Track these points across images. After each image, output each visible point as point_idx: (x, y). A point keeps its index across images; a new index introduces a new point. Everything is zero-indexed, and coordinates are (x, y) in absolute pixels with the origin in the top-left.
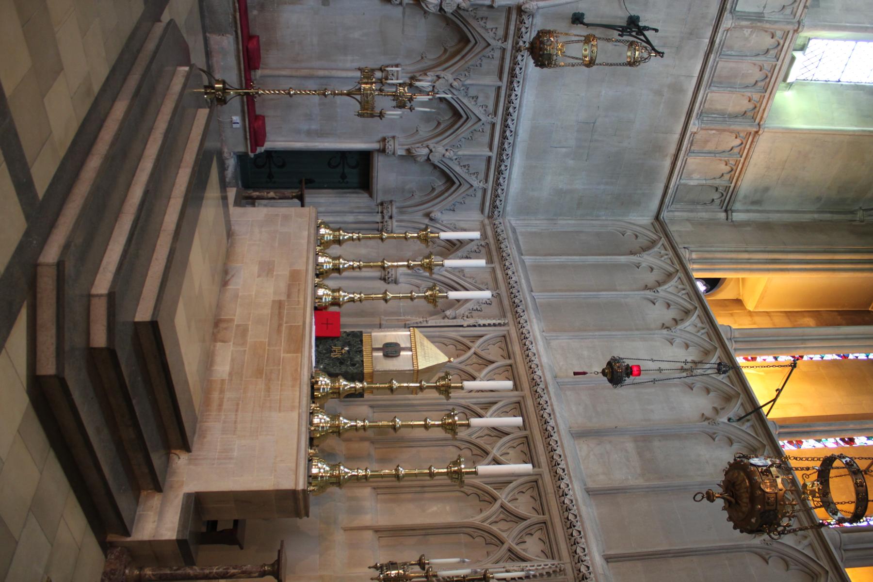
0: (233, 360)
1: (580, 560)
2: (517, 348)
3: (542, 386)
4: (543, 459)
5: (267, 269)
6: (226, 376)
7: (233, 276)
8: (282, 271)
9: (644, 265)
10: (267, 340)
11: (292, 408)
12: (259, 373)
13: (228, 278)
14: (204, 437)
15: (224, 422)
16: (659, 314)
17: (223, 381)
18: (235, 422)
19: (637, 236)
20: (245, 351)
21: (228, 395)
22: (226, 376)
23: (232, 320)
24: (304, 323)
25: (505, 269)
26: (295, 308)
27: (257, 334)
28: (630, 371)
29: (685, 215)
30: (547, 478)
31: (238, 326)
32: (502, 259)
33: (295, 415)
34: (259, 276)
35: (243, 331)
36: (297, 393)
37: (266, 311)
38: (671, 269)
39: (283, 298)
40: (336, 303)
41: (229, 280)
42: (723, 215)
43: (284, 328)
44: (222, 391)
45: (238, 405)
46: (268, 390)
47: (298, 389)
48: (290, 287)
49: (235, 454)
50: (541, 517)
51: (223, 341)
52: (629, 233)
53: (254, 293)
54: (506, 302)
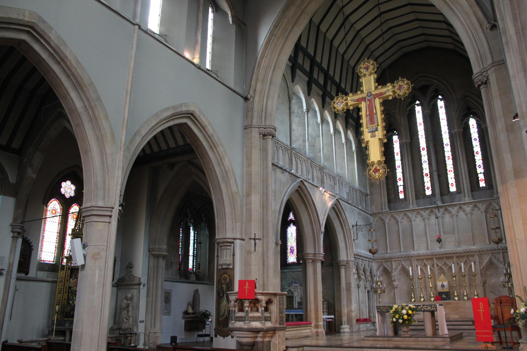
1: (476, 251)
2: (421, 258)
3: (433, 253)
9: (388, 222)
16: (405, 222)
19: (377, 221)
21: (463, 315)
22: (458, 316)
25: (395, 258)
28: (439, 238)
29: (369, 207)
30: (457, 255)
32: (392, 258)
38: (390, 215)
40: (433, 297)
42: (369, 197)
50: (465, 256)
52: (375, 223)
54: (406, 259)
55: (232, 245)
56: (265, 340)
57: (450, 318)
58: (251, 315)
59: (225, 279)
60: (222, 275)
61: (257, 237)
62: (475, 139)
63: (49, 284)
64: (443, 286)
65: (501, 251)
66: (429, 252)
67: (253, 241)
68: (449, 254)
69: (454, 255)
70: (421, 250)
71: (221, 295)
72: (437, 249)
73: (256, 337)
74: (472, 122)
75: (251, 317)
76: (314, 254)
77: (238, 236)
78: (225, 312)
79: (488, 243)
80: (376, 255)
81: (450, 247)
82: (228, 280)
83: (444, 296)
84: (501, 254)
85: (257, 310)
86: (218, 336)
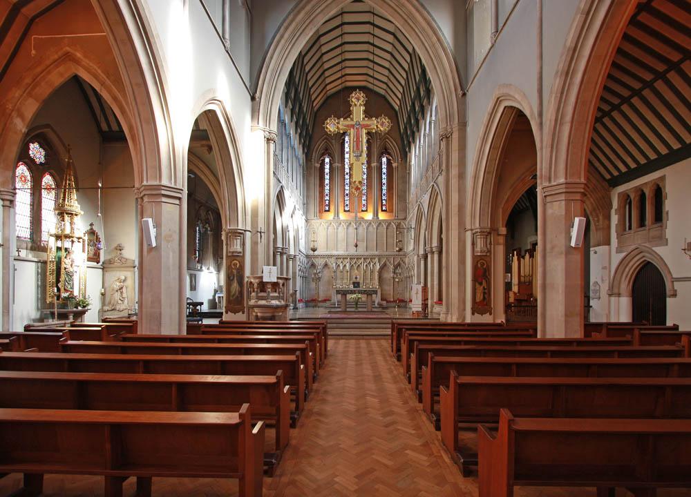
55: (242, 235)
56: (277, 314)
58: (271, 295)
59: (235, 265)
60: (231, 262)
61: (262, 231)
62: (384, 174)
63: (34, 264)
64: (356, 278)
66: (346, 253)
67: (259, 234)
70: (341, 252)
71: (232, 278)
72: (352, 251)
73: (273, 312)
74: (384, 160)
75: (272, 297)
76: (283, 249)
77: (247, 229)
78: (235, 292)
80: (316, 253)
81: (361, 251)
82: (238, 266)
83: (356, 285)
85: (276, 292)
86: (229, 313)
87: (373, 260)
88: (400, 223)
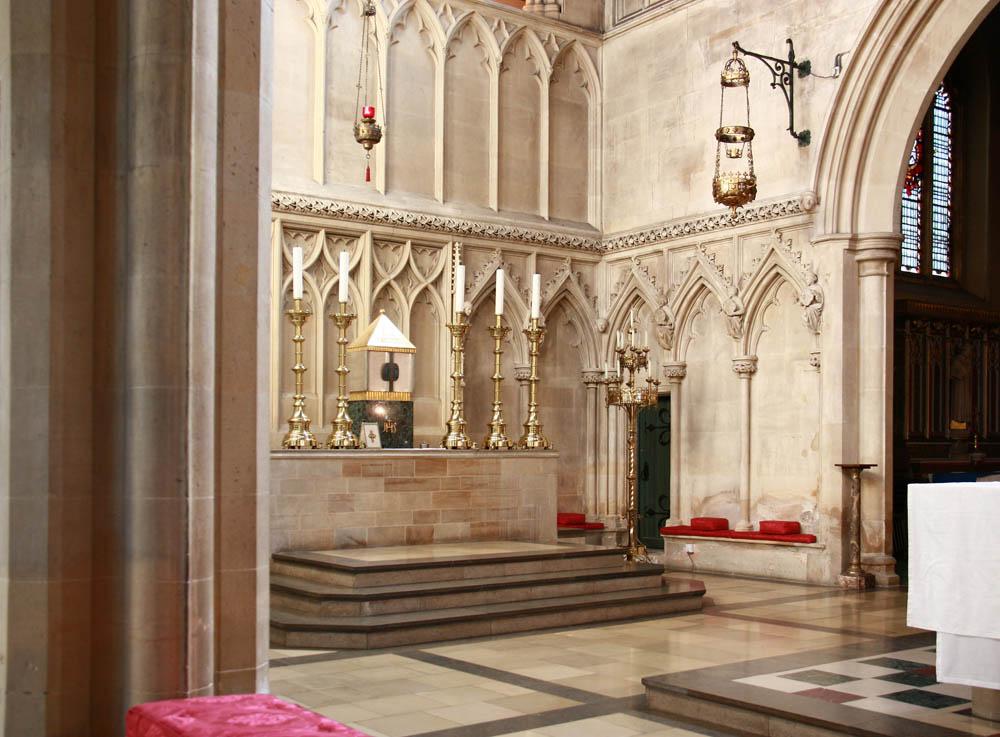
0: (452, 521)
4: (359, 226)
5: (342, 502)
6: (468, 524)
7: (351, 538)
8: (346, 485)
10: (431, 492)
11: (498, 463)
12: (465, 495)
13: (353, 543)
14: (519, 532)
15: (508, 518)
17: (472, 526)
18: (508, 509)
20: (443, 511)
21: (485, 519)
22: (468, 524)
23: (409, 531)
24: (414, 458)
26: (395, 468)
27: (424, 501)
30: (379, 229)
31: (415, 522)
33: (503, 461)
34: (352, 510)
35: (422, 516)
36: (486, 460)
37: (398, 497)
39: (382, 481)
41: (357, 541)
43: (420, 477)
44: (482, 525)
45: (494, 510)
46: (481, 485)
47: (481, 460)
48: (367, 475)
49: (532, 505)
51: (433, 532)
53: (375, 512)
57: (435, 537)
65: (535, 250)
68: (350, 218)
69: (370, 228)
79: (496, 209)
84: (533, 257)
87: (426, 259)
88: (568, 50)
